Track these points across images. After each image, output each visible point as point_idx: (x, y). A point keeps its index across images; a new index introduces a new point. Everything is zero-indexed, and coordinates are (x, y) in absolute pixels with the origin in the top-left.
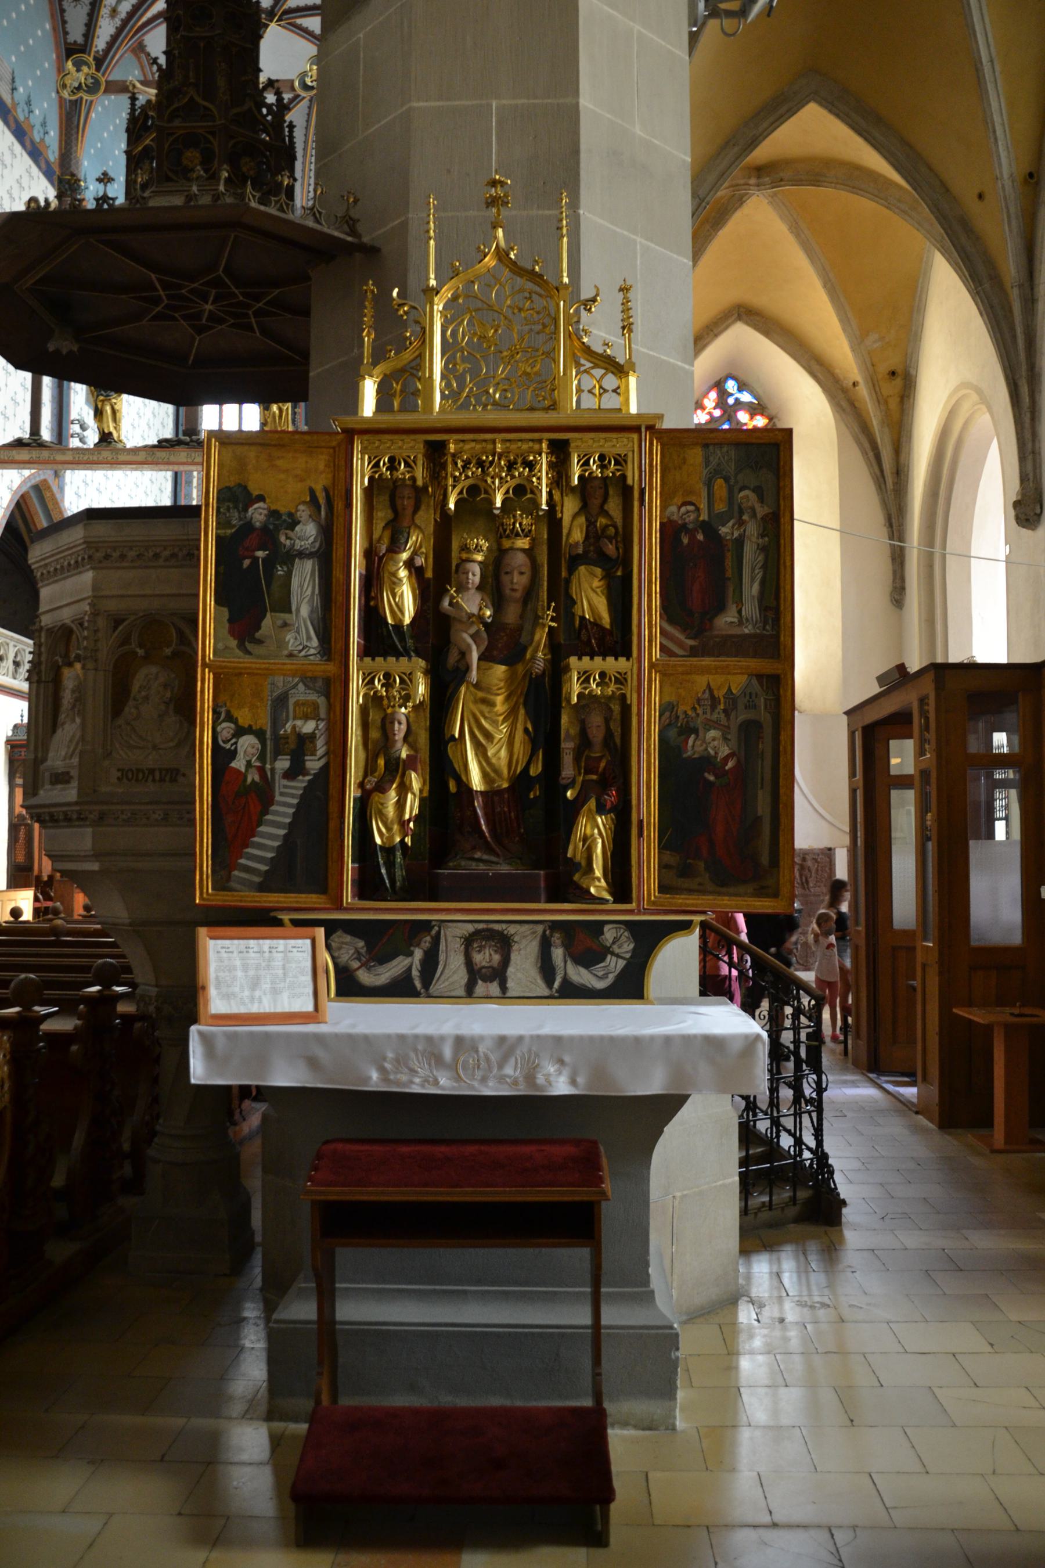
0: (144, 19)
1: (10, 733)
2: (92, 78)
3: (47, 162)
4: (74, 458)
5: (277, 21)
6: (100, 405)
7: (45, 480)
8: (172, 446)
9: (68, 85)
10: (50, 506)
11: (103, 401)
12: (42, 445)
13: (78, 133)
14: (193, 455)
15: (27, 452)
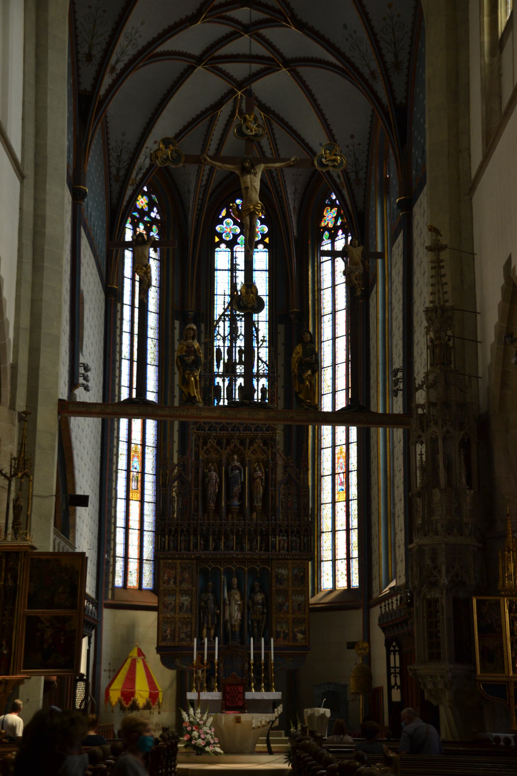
2: (176, 153)
5: (204, 65)
6: (187, 376)
9: (159, 157)
11: (189, 374)
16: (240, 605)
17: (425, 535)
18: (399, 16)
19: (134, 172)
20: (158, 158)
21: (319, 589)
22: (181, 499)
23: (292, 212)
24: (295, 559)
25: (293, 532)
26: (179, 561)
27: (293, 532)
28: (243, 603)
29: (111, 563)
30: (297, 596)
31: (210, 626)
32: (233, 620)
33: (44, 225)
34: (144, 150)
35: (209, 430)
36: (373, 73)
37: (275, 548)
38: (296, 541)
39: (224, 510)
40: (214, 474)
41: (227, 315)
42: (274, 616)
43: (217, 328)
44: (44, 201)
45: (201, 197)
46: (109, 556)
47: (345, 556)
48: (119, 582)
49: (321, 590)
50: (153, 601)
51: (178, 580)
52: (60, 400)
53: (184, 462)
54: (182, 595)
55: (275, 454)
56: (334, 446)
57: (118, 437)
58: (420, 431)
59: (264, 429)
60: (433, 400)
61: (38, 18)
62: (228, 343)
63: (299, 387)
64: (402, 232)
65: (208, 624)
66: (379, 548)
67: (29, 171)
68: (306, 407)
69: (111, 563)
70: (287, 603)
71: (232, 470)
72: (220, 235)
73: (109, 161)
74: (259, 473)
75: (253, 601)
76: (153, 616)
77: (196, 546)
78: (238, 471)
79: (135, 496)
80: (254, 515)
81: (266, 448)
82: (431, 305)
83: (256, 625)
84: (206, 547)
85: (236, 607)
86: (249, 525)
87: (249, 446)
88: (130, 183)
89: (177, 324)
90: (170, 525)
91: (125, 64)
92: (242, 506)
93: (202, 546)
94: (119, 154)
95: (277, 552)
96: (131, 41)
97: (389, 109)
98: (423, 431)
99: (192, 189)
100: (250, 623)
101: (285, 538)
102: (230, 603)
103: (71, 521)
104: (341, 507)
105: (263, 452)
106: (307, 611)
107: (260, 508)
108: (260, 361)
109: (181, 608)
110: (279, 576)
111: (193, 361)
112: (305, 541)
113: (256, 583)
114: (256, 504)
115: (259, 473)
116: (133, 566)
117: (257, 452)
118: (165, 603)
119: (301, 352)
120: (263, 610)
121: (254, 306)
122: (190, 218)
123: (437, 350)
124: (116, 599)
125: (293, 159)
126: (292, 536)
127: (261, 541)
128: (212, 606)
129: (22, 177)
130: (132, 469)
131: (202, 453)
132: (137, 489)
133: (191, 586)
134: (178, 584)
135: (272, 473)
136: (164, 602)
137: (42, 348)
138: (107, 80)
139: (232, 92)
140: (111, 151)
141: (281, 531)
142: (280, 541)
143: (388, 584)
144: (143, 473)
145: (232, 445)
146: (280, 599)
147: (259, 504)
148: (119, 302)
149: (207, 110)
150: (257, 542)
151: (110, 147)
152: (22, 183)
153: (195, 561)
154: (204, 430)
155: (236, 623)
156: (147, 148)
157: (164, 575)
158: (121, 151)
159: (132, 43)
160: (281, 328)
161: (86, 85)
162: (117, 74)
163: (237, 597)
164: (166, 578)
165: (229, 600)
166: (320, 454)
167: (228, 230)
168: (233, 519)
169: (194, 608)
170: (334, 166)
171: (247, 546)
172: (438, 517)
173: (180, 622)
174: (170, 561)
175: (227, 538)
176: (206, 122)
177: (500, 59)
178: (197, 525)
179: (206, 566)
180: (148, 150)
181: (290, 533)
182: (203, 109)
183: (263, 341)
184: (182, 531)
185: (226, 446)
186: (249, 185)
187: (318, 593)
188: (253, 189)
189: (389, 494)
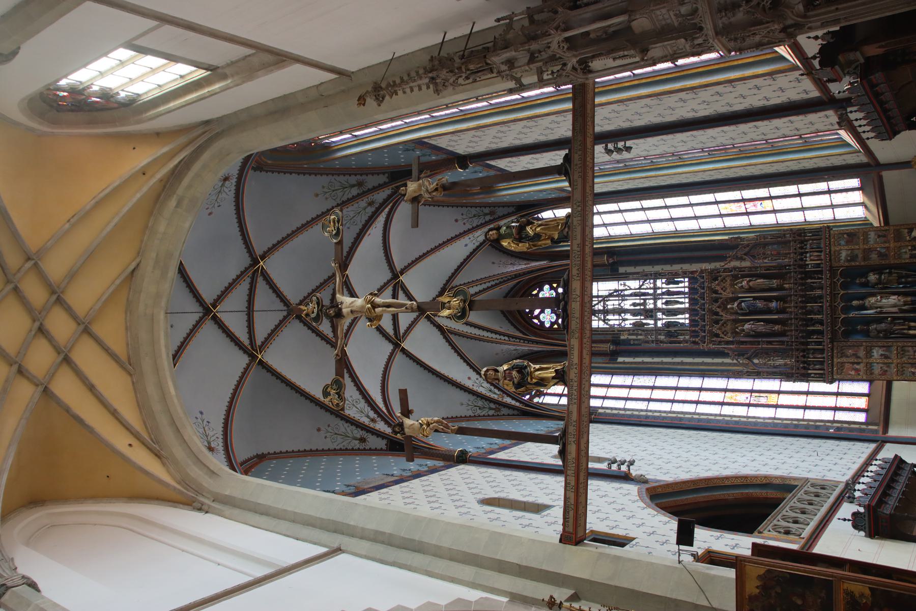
0: (385, 411)
1: (862, 533)
3: (442, 467)
4: (575, 403)
6: (534, 381)
7: (647, 489)
8: (567, 316)
10: (670, 490)
11: (532, 379)
12: (564, 432)
13: (433, 449)
14: (574, 296)
15: (569, 446)
16: (881, 297)
17: (701, 29)
18: (323, 187)
19: (493, 396)
20: (338, 404)
21: (866, 219)
22: (772, 358)
23: (528, 266)
24: (830, 244)
25: (801, 248)
26: (835, 360)
27: (801, 248)
28: (879, 293)
29: (839, 425)
30: (869, 240)
31: (907, 327)
32: (899, 303)
33: (383, 533)
34: (475, 388)
35: (705, 333)
36: (370, 204)
37: (819, 264)
38: (811, 244)
39: (781, 316)
40: (747, 326)
41: (604, 317)
42: (892, 262)
43: (616, 326)
44: (363, 529)
45: (518, 340)
46: (832, 427)
47: (827, 196)
48: (861, 417)
49: (865, 218)
50: (880, 385)
51: (856, 361)
52: (561, 541)
53: (736, 355)
54: (871, 356)
55: (725, 269)
56: (721, 216)
57: (716, 415)
58: (565, 68)
59: (702, 280)
60: (526, 60)
61: (239, 507)
62: (628, 316)
63: (545, 239)
64: (488, 162)
65: (904, 329)
66: (811, 158)
67: (336, 540)
68: (566, 229)
69: (839, 425)
70: (878, 249)
71: (742, 309)
72: (552, 324)
73: (484, 416)
74: (744, 283)
75: (877, 284)
76: (896, 385)
77: (820, 343)
78: (743, 304)
79: (773, 399)
80: (786, 286)
81: (719, 278)
82: (431, 86)
83: (903, 280)
84: (820, 333)
85: (884, 301)
86: (796, 291)
87: (718, 294)
88: (500, 399)
89: (620, 359)
90: (798, 369)
91: (371, 410)
92: (777, 299)
93: (819, 337)
94: (478, 408)
95: (823, 262)
96: (353, 405)
97: (394, 186)
98: (565, 65)
99: (514, 348)
100: (901, 286)
101: (808, 255)
102: (880, 308)
103: (777, 482)
104: (779, 204)
105: (724, 281)
106: (886, 228)
107: (779, 281)
108: (642, 287)
109: (886, 357)
110: (849, 258)
111: (518, 372)
112: (810, 235)
113: (857, 281)
114: (775, 285)
115: (744, 283)
116: (843, 402)
117: (724, 287)
118: (881, 373)
119: (508, 241)
120: (886, 273)
121: (461, 300)
122: (535, 349)
123: (472, 67)
124: (877, 421)
125: (333, 265)
126: (806, 249)
127: (812, 278)
128: (883, 325)
129: (338, 551)
130: (748, 402)
131: (727, 338)
132: (767, 397)
133: (862, 348)
134: (860, 361)
135: (744, 271)
136: (880, 375)
137: (498, 557)
138: (381, 426)
139: (428, 318)
140: (476, 414)
141: (801, 260)
142: (811, 260)
143: (848, 145)
144: (752, 391)
145: (718, 310)
146: (874, 256)
147: (775, 283)
148: (597, 411)
149: (445, 337)
150: (813, 283)
151: (473, 415)
152: (344, 552)
153: (835, 343)
154: (704, 337)
155: (902, 301)
156: (473, 385)
157: (850, 374)
158: (475, 406)
159: (355, 404)
160: (622, 270)
161: (381, 444)
163: (872, 300)
164: (853, 373)
165: (877, 308)
166: (730, 229)
167: (548, 317)
168: (790, 307)
169: (885, 344)
170: (338, 222)
171: (819, 292)
172: (672, 13)
173: (902, 358)
174: (835, 369)
175: (811, 312)
176: (452, 337)
177: (223, 67)
178: (796, 342)
179: (840, 332)
180: (475, 384)
181: (803, 251)
182: (444, 341)
183: (625, 285)
184: (804, 356)
185: (719, 316)
186: (349, 309)
187: (868, 220)
188: (352, 305)
189: (753, 154)
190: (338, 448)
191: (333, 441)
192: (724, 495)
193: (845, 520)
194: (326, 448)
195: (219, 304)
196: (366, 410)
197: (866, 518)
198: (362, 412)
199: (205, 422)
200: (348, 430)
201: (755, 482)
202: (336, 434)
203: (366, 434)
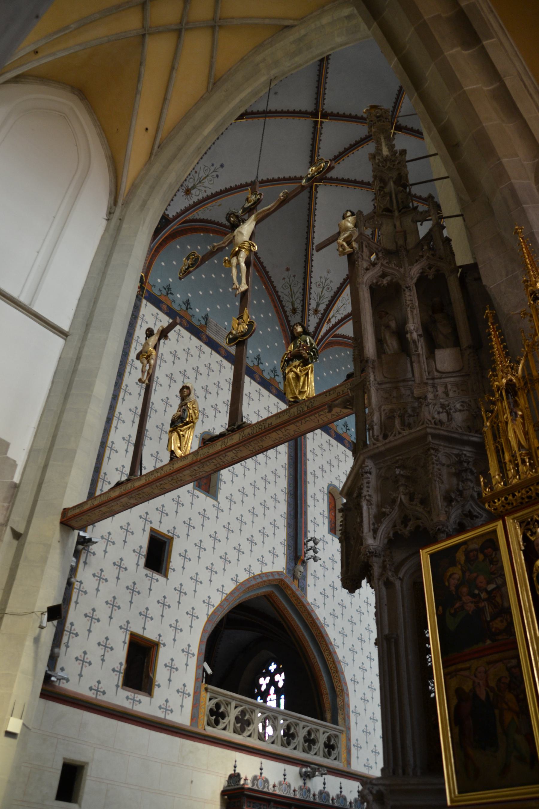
10: (295, 602)
14: (226, 441)
91: (327, 305)
96: (324, 287)
159: (325, 288)
162: (322, 314)
190: (280, 294)
191: (284, 286)
192: (313, 653)
193: (235, 767)
194: (275, 284)
195: (330, 119)
196: (324, 301)
197: (236, 787)
198: (320, 298)
199: (214, 174)
200: (298, 294)
201: (334, 681)
202: (290, 286)
203: (300, 312)
